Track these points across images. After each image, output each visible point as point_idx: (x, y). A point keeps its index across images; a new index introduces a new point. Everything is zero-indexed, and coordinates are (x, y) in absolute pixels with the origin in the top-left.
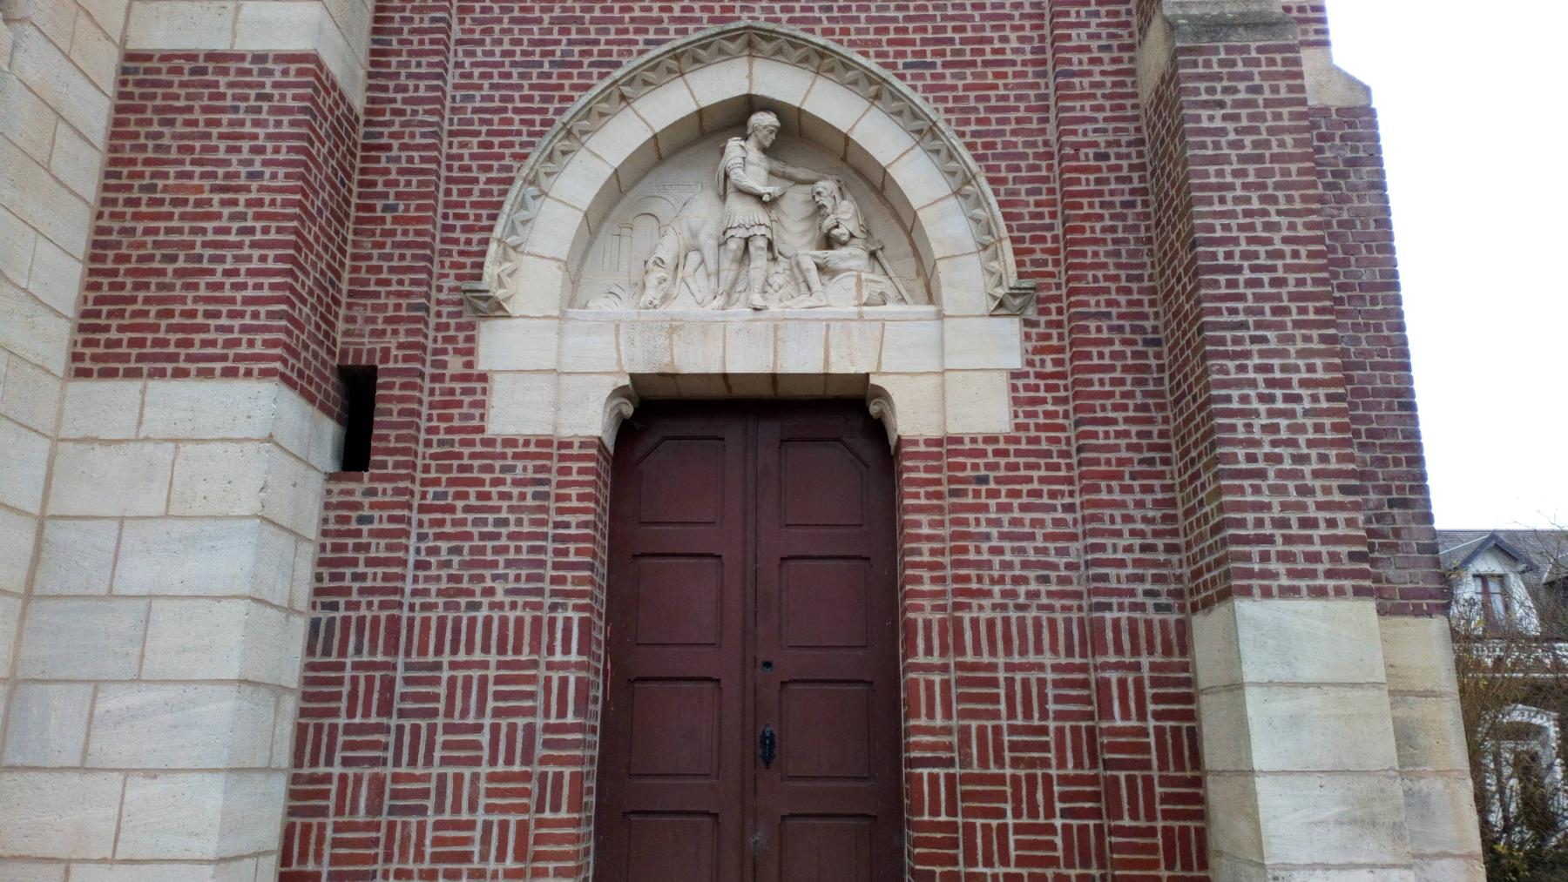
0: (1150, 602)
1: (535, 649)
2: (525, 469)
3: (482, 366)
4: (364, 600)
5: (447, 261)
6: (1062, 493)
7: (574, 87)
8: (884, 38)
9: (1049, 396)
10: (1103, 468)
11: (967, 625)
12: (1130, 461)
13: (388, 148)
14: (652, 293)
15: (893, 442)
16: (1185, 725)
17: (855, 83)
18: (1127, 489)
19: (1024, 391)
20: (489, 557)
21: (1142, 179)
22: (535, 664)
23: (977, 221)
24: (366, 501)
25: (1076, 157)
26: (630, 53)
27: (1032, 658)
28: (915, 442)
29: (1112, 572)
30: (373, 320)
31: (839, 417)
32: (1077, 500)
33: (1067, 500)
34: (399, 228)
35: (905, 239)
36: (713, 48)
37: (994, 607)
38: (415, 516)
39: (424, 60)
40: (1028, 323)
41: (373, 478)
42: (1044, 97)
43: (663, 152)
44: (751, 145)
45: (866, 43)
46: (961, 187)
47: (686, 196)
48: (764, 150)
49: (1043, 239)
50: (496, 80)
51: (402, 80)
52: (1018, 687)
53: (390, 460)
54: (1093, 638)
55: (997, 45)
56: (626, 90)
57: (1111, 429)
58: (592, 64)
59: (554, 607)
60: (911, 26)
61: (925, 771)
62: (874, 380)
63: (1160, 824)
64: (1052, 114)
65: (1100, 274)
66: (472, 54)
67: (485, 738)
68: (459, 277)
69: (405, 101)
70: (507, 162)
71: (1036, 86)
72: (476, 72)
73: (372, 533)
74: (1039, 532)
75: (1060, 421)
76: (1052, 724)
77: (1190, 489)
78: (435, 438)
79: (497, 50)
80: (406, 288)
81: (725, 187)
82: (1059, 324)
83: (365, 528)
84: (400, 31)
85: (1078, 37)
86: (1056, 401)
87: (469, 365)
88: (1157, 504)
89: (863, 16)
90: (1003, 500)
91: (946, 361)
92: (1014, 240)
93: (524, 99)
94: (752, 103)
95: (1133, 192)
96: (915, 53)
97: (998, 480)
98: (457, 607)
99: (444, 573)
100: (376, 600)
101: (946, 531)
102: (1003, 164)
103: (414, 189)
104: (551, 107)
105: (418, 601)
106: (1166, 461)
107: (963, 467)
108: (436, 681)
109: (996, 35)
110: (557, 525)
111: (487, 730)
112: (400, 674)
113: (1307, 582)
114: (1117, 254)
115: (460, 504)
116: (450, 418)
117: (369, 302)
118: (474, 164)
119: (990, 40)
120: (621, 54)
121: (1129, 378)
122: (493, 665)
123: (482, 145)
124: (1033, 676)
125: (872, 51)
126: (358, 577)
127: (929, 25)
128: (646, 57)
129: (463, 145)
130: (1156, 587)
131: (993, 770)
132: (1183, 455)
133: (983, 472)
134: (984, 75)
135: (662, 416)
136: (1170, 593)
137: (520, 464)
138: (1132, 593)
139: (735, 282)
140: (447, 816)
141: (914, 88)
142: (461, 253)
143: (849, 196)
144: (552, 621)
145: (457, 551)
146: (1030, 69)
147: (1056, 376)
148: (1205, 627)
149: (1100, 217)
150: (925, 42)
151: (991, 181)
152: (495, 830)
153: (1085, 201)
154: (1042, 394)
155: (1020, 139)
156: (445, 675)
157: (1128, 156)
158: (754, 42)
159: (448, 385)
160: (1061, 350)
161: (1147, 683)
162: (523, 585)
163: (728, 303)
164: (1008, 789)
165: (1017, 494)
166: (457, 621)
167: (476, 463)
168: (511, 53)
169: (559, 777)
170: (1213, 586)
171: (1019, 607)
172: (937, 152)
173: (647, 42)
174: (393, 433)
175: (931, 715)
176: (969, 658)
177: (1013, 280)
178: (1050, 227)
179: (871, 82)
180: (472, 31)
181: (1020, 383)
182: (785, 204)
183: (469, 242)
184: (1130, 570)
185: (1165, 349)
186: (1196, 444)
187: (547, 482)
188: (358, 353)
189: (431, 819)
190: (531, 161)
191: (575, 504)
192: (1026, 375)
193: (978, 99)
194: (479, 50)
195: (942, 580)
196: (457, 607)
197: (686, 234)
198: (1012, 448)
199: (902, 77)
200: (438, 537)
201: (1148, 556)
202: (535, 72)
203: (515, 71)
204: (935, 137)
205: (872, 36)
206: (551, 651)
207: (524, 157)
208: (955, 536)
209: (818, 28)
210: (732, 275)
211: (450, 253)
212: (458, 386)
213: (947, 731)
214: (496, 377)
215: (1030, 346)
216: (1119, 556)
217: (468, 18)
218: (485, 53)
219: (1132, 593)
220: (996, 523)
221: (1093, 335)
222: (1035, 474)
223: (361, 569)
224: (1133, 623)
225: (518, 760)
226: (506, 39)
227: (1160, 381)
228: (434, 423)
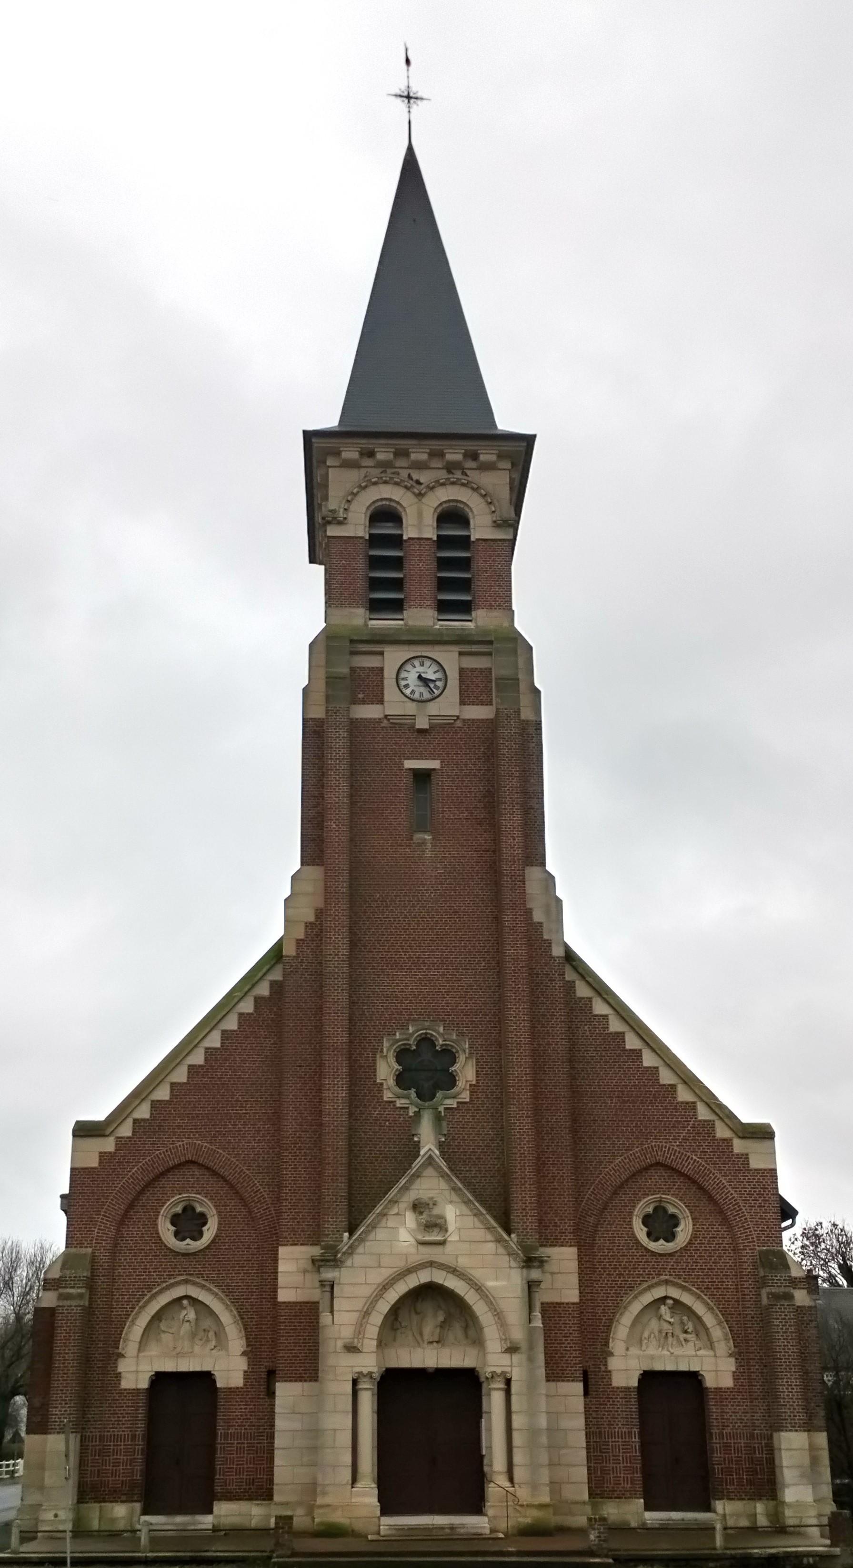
19: (736, 1376)
46: (720, 1323)
62: (701, 1373)
91: (717, 1368)
94: (666, 1298)
135: (651, 1379)
148: (775, 1435)
177: (733, 1348)
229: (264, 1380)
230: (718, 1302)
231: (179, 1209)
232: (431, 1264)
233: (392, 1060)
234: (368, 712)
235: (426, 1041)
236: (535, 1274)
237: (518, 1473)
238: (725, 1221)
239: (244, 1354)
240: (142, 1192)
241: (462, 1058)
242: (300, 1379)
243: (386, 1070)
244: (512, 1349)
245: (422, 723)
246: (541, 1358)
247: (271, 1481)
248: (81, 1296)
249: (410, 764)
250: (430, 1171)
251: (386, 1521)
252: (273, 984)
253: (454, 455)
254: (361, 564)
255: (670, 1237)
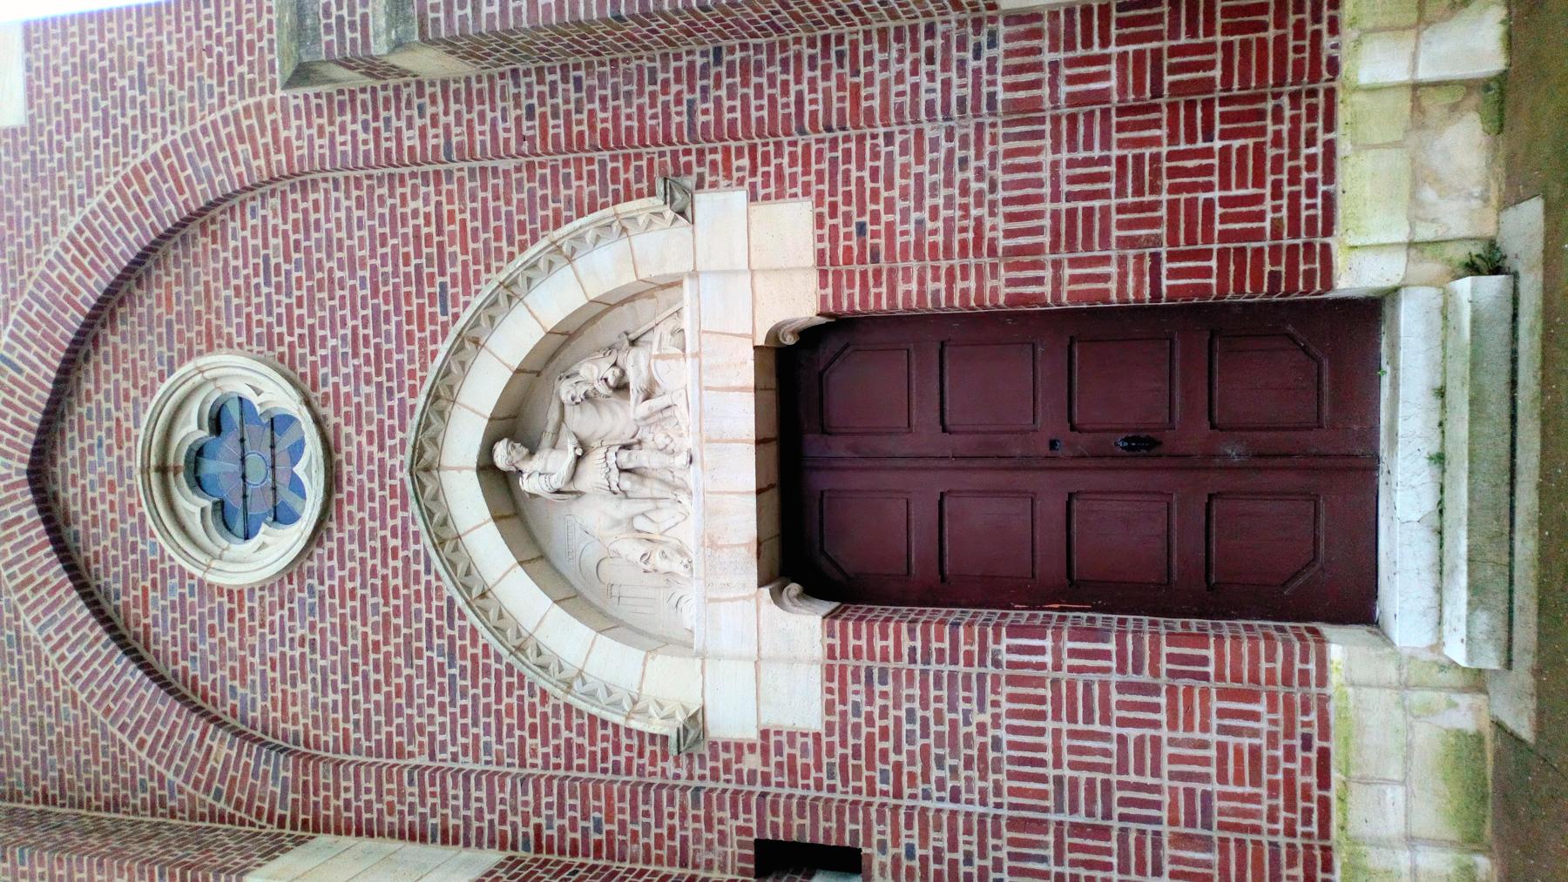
0: (986, 53)
1: (1040, 682)
2: (856, 692)
3: (753, 735)
4: (991, 854)
5: (649, 769)
6: (874, 146)
7: (474, 643)
8: (417, 335)
9: (774, 162)
10: (847, 104)
11: (1012, 242)
12: (840, 77)
13: (538, 828)
14: (676, 565)
15: (823, 320)
16: (1114, 14)
17: (463, 364)
18: (869, 79)
20: (946, 728)
21: (552, 71)
22: (1055, 682)
23: (598, 238)
24: (891, 851)
25: (532, 139)
26: (438, 588)
27: (1045, 174)
28: (824, 299)
29: (955, 93)
30: (710, 843)
31: (798, 375)
32: (881, 130)
33: (881, 140)
34: (617, 817)
35: (617, 310)
36: (433, 507)
37: (992, 214)
38: (906, 802)
39: (451, 792)
40: (700, 185)
41: (868, 844)
42: (472, 171)
43: (535, 554)
44: (526, 467)
45: (423, 353)
47: (579, 532)
48: (532, 453)
49: (615, 171)
50: (469, 721)
51: (471, 813)
52: (1076, 188)
53: (849, 827)
54: (1024, 112)
55: (421, 221)
56: (476, 592)
57: (807, 97)
58: (451, 626)
59: (996, 663)
60: (405, 308)
61: (1165, 283)
63: (1219, 39)
64: (488, 164)
65: (649, 112)
66: (443, 744)
67: (1132, 733)
68: (665, 757)
69: (492, 811)
70: (549, 710)
71: (461, 181)
72: (461, 740)
73: (924, 844)
74: (915, 169)
75: (799, 150)
76: (1115, 152)
77: (869, 15)
78: (826, 782)
79: (439, 719)
80: (677, 810)
81: (568, 493)
82: (701, 153)
83: (918, 852)
84: (423, 816)
85: (411, 139)
86: (779, 154)
87: (752, 748)
88: (884, 47)
89: (396, 357)
90: (881, 207)
91: (738, 268)
92: (616, 201)
93: (486, 693)
95: (565, 80)
96: (432, 304)
97: (861, 212)
98: (997, 761)
99: (963, 773)
100: (991, 841)
101: (914, 264)
102: (540, 213)
103: (578, 802)
104: (494, 666)
105: (992, 800)
106: (840, 39)
107: (848, 249)
108: (1074, 783)
109: (411, 222)
110: (913, 660)
111: (1124, 731)
112: (1066, 818)
114: (628, 94)
115: (893, 757)
116: (806, 767)
117: (691, 846)
118: (553, 742)
119: (417, 228)
120: (440, 598)
121: (754, 80)
122: (1057, 725)
123: (533, 735)
124: (1064, 172)
125: (430, 348)
126: (968, 860)
127: (404, 290)
128: (443, 573)
129: (534, 753)
130: (971, 46)
131: (1163, 212)
132: (833, 22)
133: (853, 229)
134: (452, 234)
136: (977, 32)
137: (851, 698)
138: (977, 72)
139: (662, 481)
140: (1213, 770)
141: (466, 304)
142: (641, 755)
143: (575, 368)
144: (1011, 665)
145: (940, 760)
146: (444, 187)
147: (756, 155)
149: (592, 113)
150: (420, 294)
151: (557, 225)
152: (1227, 722)
153: (575, 129)
154: (772, 169)
155: (515, 197)
156: (1067, 772)
157: (529, 85)
158: (424, 466)
159: (772, 769)
160: (727, 150)
161: (1071, 55)
162: (974, 695)
163: (685, 488)
164: (1183, 196)
165: (875, 194)
166: (1012, 760)
167: (851, 741)
168: (442, 706)
169: (1172, 658)
171: (993, 187)
172: (529, 280)
173: (428, 571)
174: (822, 824)
175: (1105, 278)
176: (1046, 239)
177: (657, 201)
178: (603, 163)
179: (461, 348)
180: (421, 745)
181: (761, 192)
182: (585, 433)
183: (629, 748)
184: (954, 74)
185: (724, 43)
186: (823, 10)
187: (869, 671)
188: (743, 858)
189: (1215, 787)
190: (548, 687)
191: (891, 643)
192: (753, 186)
193: (475, 240)
194: (439, 738)
195: (964, 268)
196: (997, 761)
197: (616, 531)
198: (827, 199)
199: (456, 317)
200: (926, 780)
201: (938, 57)
202: (460, 682)
203: (460, 702)
204: (515, 283)
205: (416, 347)
206: (1042, 666)
207: (544, 693)
208: (919, 256)
209: (410, 402)
210: (656, 485)
211: (641, 767)
212: (773, 759)
213: (1122, 261)
214: (764, 721)
215: (723, 183)
216: (938, 85)
217: (408, 749)
218: (443, 732)
219: (977, 72)
220: (905, 213)
221: (711, 117)
222: (854, 174)
223: (960, 856)
224: (1008, 71)
225: (1154, 699)
226: (428, 711)
227: (757, 48)
228: (811, 782)
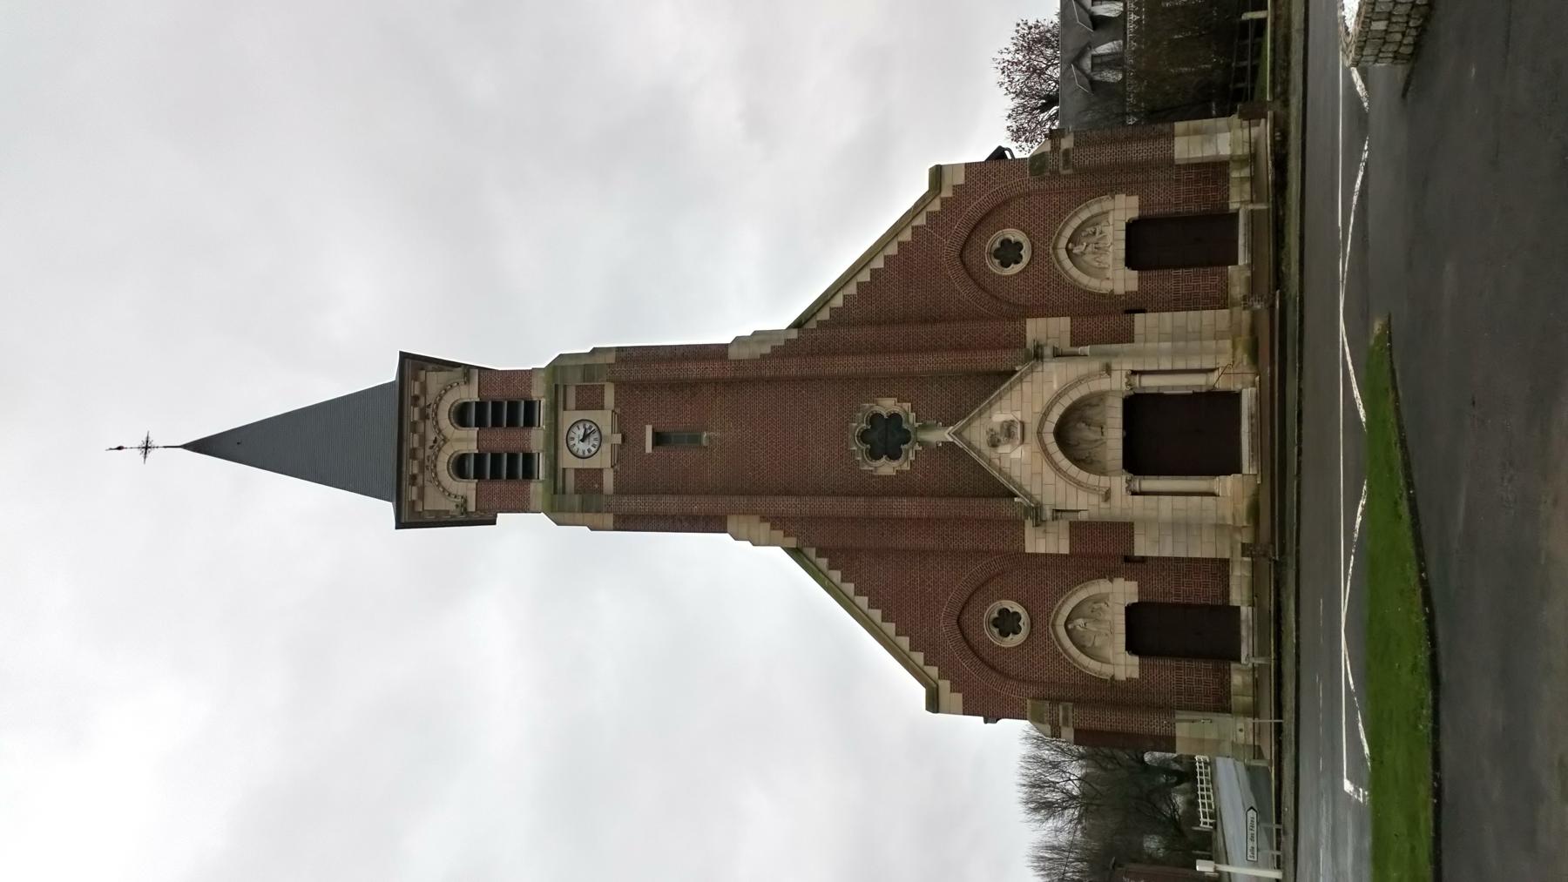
81: (1083, 253)
91: (1123, 209)
113: (1172, 148)
135: (1131, 262)
170: (1170, 162)
229: (1131, 564)
230: (1070, 208)
231: (996, 631)
232: (1040, 433)
233: (878, 463)
234: (608, 480)
235: (863, 436)
236: (1048, 351)
237: (1208, 365)
238: (1006, 203)
239: (1111, 580)
240: (982, 660)
241: (877, 409)
242: (1132, 536)
243: (886, 468)
244: (1108, 370)
245: (618, 439)
246: (1115, 347)
247: (1213, 560)
248: (1065, 709)
249: (649, 449)
250: (966, 434)
251: (1245, 469)
252: (819, 555)
253: (415, 414)
254: (498, 486)
255: (1019, 246)
